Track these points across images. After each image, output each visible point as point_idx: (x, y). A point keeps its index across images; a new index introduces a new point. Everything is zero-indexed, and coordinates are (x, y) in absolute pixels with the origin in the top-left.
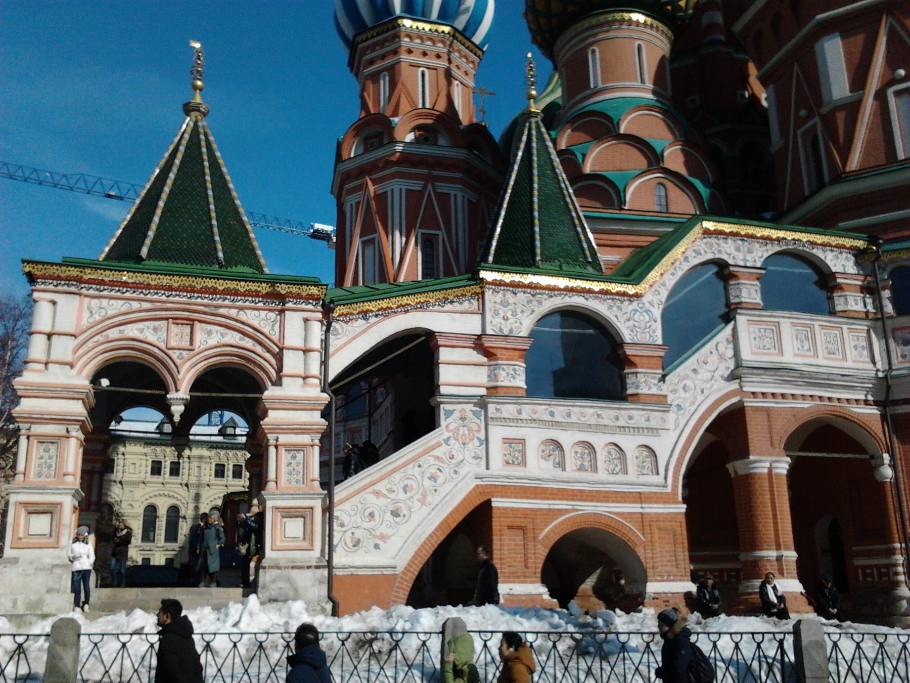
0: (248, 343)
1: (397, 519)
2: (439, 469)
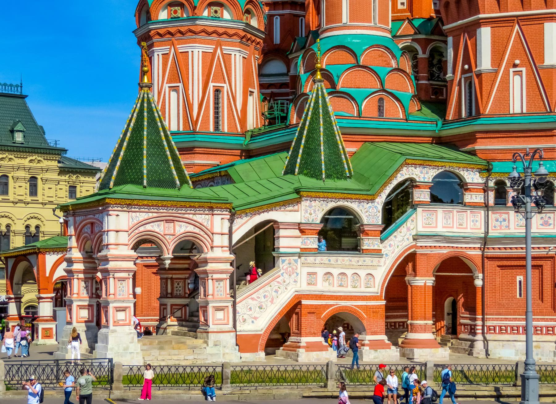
0: (197, 230)
1: (261, 310)
2: (279, 287)
